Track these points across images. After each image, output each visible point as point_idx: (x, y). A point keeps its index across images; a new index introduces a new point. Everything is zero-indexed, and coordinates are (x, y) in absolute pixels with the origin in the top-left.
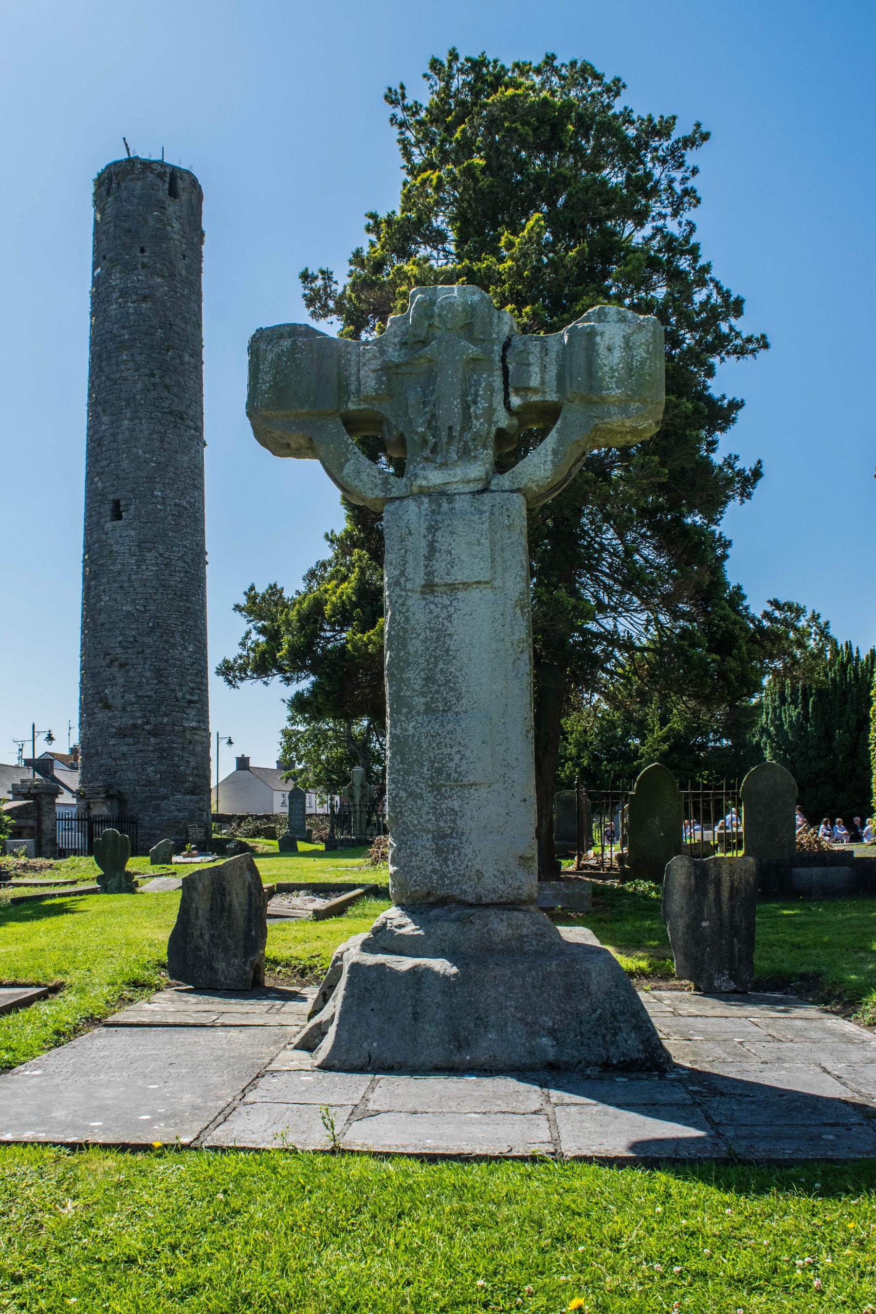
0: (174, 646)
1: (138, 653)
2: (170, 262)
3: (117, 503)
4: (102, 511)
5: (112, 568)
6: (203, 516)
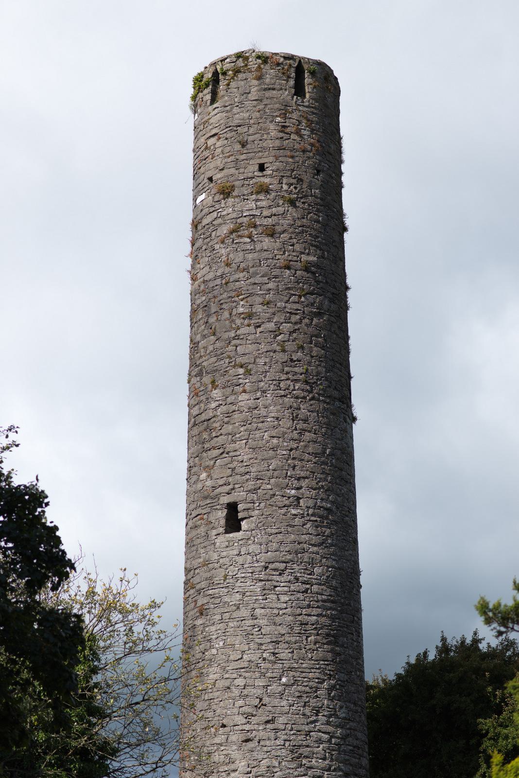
1: (268, 722)
3: (232, 508)
4: (212, 518)
5: (226, 599)
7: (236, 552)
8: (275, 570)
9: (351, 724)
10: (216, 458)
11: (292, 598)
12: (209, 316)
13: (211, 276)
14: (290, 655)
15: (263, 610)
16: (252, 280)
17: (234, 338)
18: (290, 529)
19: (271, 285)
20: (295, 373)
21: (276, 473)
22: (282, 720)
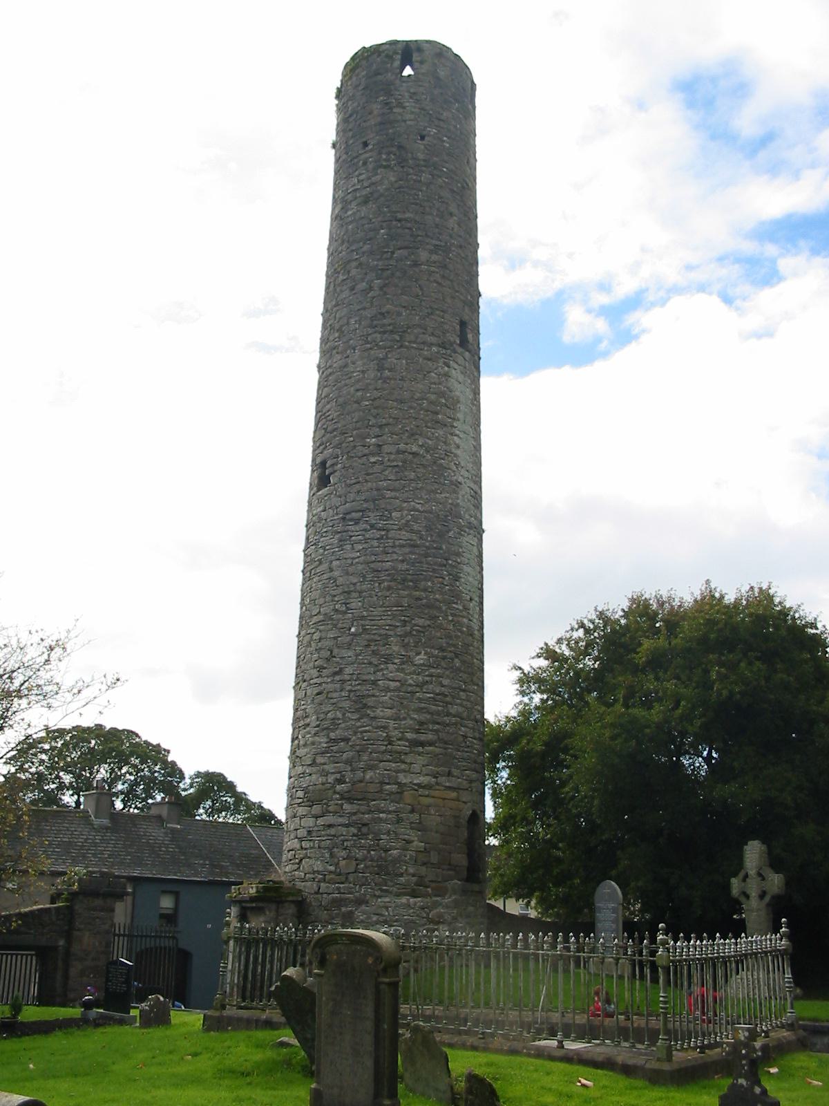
0: (388, 659)
1: (336, 674)
2: (400, 147)
7: (321, 508)
8: (351, 520)
9: (433, 670)
14: (360, 604)
15: (338, 562)
18: (367, 478)
19: (366, 248)
20: (384, 325)
21: (359, 425)
22: (349, 670)
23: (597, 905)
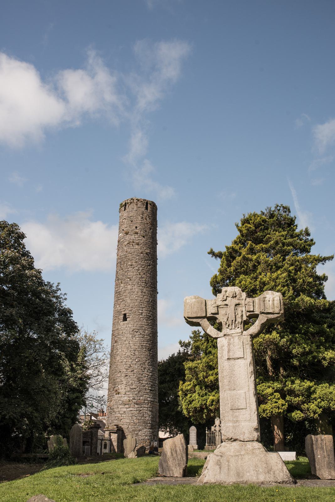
1: (132, 371)
3: (125, 315)
4: (119, 318)
5: (122, 339)
6: (157, 319)
8: (135, 331)
9: (154, 372)
10: (121, 302)
11: (139, 339)
12: (121, 265)
13: (122, 255)
15: (132, 342)
16: (132, 256)
17: (127, 271)
18: (139, 321)
19: (137, 258)
22: (136, 371)
23: (190, 432)
